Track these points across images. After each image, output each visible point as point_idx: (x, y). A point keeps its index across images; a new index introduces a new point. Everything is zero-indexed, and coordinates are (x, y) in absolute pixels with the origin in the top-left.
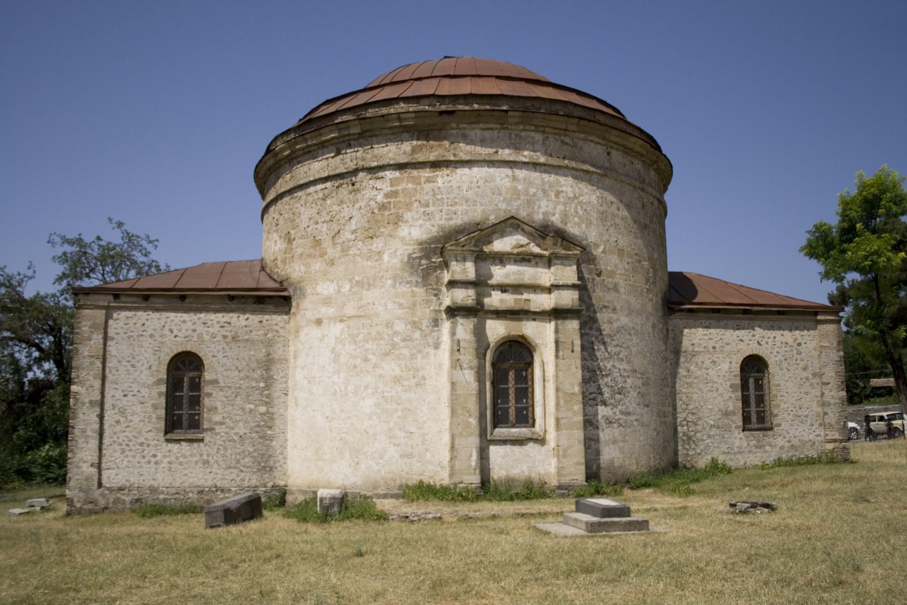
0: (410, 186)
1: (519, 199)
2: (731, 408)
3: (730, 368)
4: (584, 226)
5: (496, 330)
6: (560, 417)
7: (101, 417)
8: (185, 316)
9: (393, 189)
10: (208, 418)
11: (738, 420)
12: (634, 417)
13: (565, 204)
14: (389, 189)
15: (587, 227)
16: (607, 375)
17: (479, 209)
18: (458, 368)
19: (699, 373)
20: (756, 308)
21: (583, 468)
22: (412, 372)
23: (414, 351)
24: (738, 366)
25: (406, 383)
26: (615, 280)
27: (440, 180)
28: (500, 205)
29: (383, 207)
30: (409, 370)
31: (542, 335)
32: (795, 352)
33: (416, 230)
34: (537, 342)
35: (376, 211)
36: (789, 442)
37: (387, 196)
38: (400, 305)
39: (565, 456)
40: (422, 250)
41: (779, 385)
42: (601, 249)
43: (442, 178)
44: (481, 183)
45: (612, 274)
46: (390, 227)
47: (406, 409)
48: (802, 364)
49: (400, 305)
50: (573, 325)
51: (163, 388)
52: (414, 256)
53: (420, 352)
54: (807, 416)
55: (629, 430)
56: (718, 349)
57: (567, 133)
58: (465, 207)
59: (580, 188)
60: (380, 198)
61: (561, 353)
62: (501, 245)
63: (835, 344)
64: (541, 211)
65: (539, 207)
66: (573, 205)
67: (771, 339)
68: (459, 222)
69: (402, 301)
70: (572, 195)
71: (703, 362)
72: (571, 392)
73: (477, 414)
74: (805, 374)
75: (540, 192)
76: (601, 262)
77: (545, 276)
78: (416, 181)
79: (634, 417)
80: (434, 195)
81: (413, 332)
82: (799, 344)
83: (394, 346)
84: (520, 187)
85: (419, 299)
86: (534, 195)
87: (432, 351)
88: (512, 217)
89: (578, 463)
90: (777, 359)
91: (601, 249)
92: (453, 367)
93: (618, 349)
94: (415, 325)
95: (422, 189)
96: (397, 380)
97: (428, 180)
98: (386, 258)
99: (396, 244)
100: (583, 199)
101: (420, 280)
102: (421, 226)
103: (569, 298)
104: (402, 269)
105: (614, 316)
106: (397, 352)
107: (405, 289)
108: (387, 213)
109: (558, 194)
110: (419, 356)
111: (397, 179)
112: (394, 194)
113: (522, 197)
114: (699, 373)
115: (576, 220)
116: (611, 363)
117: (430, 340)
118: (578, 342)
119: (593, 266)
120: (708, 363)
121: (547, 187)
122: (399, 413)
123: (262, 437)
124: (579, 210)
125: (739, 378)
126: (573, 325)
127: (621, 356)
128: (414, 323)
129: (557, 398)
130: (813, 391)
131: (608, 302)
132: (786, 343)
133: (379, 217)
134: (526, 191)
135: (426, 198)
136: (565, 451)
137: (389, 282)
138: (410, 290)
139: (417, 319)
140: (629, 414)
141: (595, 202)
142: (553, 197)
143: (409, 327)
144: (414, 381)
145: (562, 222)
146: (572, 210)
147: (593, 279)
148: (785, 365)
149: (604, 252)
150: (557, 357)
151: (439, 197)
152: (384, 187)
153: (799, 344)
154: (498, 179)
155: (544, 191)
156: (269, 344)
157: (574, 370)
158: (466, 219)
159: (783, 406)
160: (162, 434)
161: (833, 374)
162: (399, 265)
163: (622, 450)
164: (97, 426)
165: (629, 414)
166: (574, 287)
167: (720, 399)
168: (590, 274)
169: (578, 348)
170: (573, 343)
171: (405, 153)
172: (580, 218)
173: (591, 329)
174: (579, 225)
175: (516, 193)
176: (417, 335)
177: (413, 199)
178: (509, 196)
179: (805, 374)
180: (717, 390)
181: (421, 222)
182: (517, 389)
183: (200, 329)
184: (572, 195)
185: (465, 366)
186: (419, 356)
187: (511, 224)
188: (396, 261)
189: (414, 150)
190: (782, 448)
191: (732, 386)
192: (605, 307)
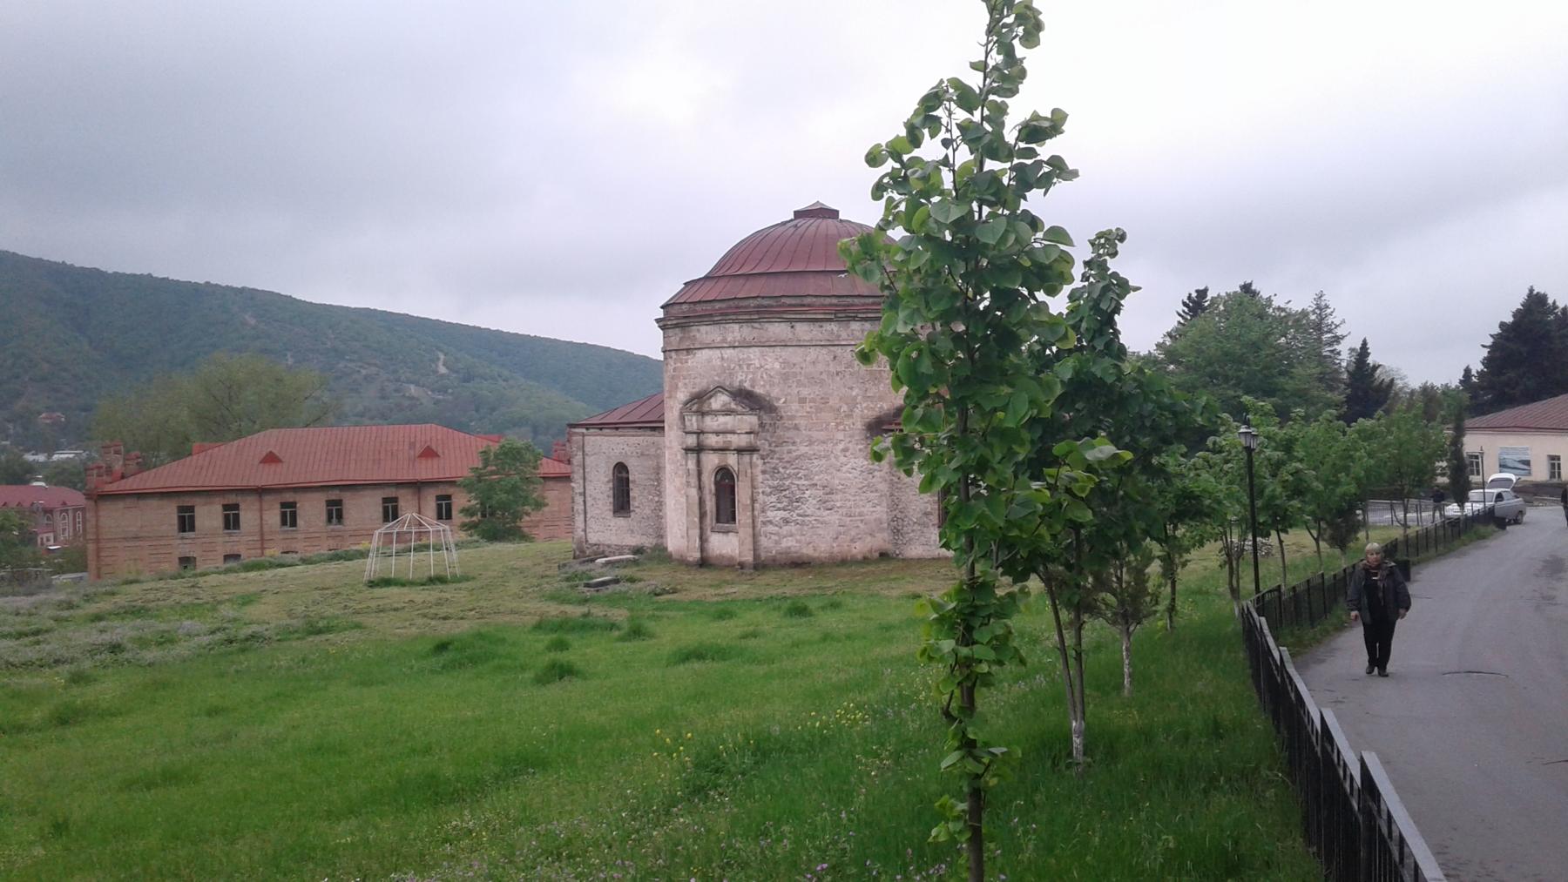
8: (618, 439)
10: (634, 504)
11: (935, 519)
45: (792, 418)
175: (724, 370)
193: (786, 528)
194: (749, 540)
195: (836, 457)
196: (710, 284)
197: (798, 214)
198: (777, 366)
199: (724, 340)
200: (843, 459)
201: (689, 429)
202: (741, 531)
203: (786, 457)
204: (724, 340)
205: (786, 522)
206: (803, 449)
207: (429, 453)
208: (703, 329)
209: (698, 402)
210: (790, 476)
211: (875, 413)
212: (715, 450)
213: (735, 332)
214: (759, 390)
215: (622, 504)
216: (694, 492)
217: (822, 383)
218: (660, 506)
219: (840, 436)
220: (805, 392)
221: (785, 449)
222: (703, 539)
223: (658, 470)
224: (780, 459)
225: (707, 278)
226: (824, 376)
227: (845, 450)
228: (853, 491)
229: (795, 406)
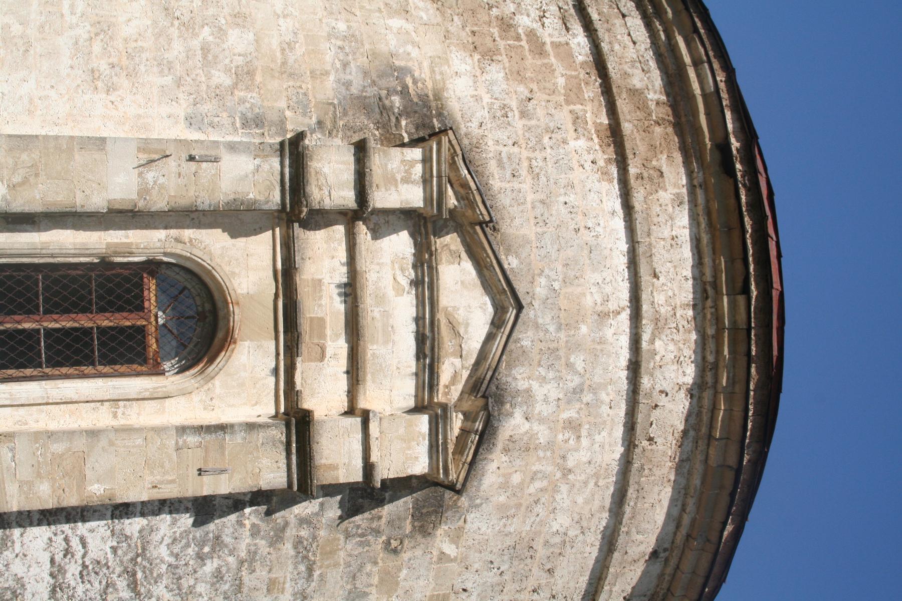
0: (561, 81)
1: (559, 329)
4: (502, 499)
5: (244, 266)
6: (19, 443)
9: (548, 47)
14: (548, 40)
15: (501, 508)
16: (133, 586)
17: (529, 231)
18: (144, 157)
22: (125, 62)
23: (179, 69)
25: (97, 47)
27: (582, 143)
28: (543, 281)
29: (506, 25)
30: (130, 57)
31: (241, 386)
33: (469, 90)
34: (217, 382)
35: (495, 12)
37: (531, 35)
38: (290, 46)
40: (424, 98)
42: (450, 549)
43: (586, 150)
44: (586, 236)
46: (465, 36)
47: (28, 45)
49: (290, 46)
50: (273, 472)
52: (409, 81)
53: (179, 83)
57: (702, 445)
58: (530, 197)
59: (586, 483)
60: (524, 22)
61: (192, 439)
62: (457, 277)
64: (535, 385)
65: (543, 380)
66: (549, 469)
69: (300, 50)
70: (570, 464)
72: (89, 473)
75: (577, 380)
76: (418, 552)
77: (392, 386)
78: (573, 94)
80: (548, 130)
81: (227, 70)
83: (189, 27)
84: (584, 329)
85: (308, 85)
86: (569, 366)
87: (182, 109)
88: (520, 307)
91: (450, 549)
92: (144, 146)
94: (244, 75)
95: (558, 106)
96: (103, 29)
97: (577, 120)
98: (396, 23)
99: (431, 46)
100: (563, 497)
101: (354, 90)
102: (477, 99)
103: (339, 455)
104: (374, 55)
106: (174, 32)
107: (330, 56)
108: (495, 31)
109: (573, 426)
110: (168, 80)
111: (570, 55)
112: (539, 49)
113: (562, 335)
115: (516, 479)
117: (206, 107)
119: (408, 528)
121: (588, 397)
122: (17, 29)
124: (538, 484)
126: (273, 472)
128: (251, 73)
129: (70, 434)
133: (483, 16)
134: (574, 346)
135: (540, 112)
137: (342, 26)
138: (328, 67)
139: (258, 78)
141: (555, 527)
142: (565, 415)
143: (240, 61)
144: (103, 66)
145: (511, 439)
146: (536, 467)
147: (377, 532)
149: (443, 557)
150: (182, 430)
151: (546, 140)
152: (548, 31)
154: (597, 277)
155: (578, 391)
157: (149, 479)
158: (504, 200)
162: (382, 48)
166: (368, 468)
168: (390, 523)
170: (223, 471)
171: (626, 75)
172: (521, 486)
173: (255, 532)
174: (505, 486)
176: (221, 78)
177: (534, 86)
178: (563, 303)
181: (487, 99)
182: (87, 332)
184: (570, 464)
185: (150, 176)
186: (168, 80)
187: (507, 300)
188: (393, 42)
192: (310, 570)
198: (561, 522)
216: (119, 185)
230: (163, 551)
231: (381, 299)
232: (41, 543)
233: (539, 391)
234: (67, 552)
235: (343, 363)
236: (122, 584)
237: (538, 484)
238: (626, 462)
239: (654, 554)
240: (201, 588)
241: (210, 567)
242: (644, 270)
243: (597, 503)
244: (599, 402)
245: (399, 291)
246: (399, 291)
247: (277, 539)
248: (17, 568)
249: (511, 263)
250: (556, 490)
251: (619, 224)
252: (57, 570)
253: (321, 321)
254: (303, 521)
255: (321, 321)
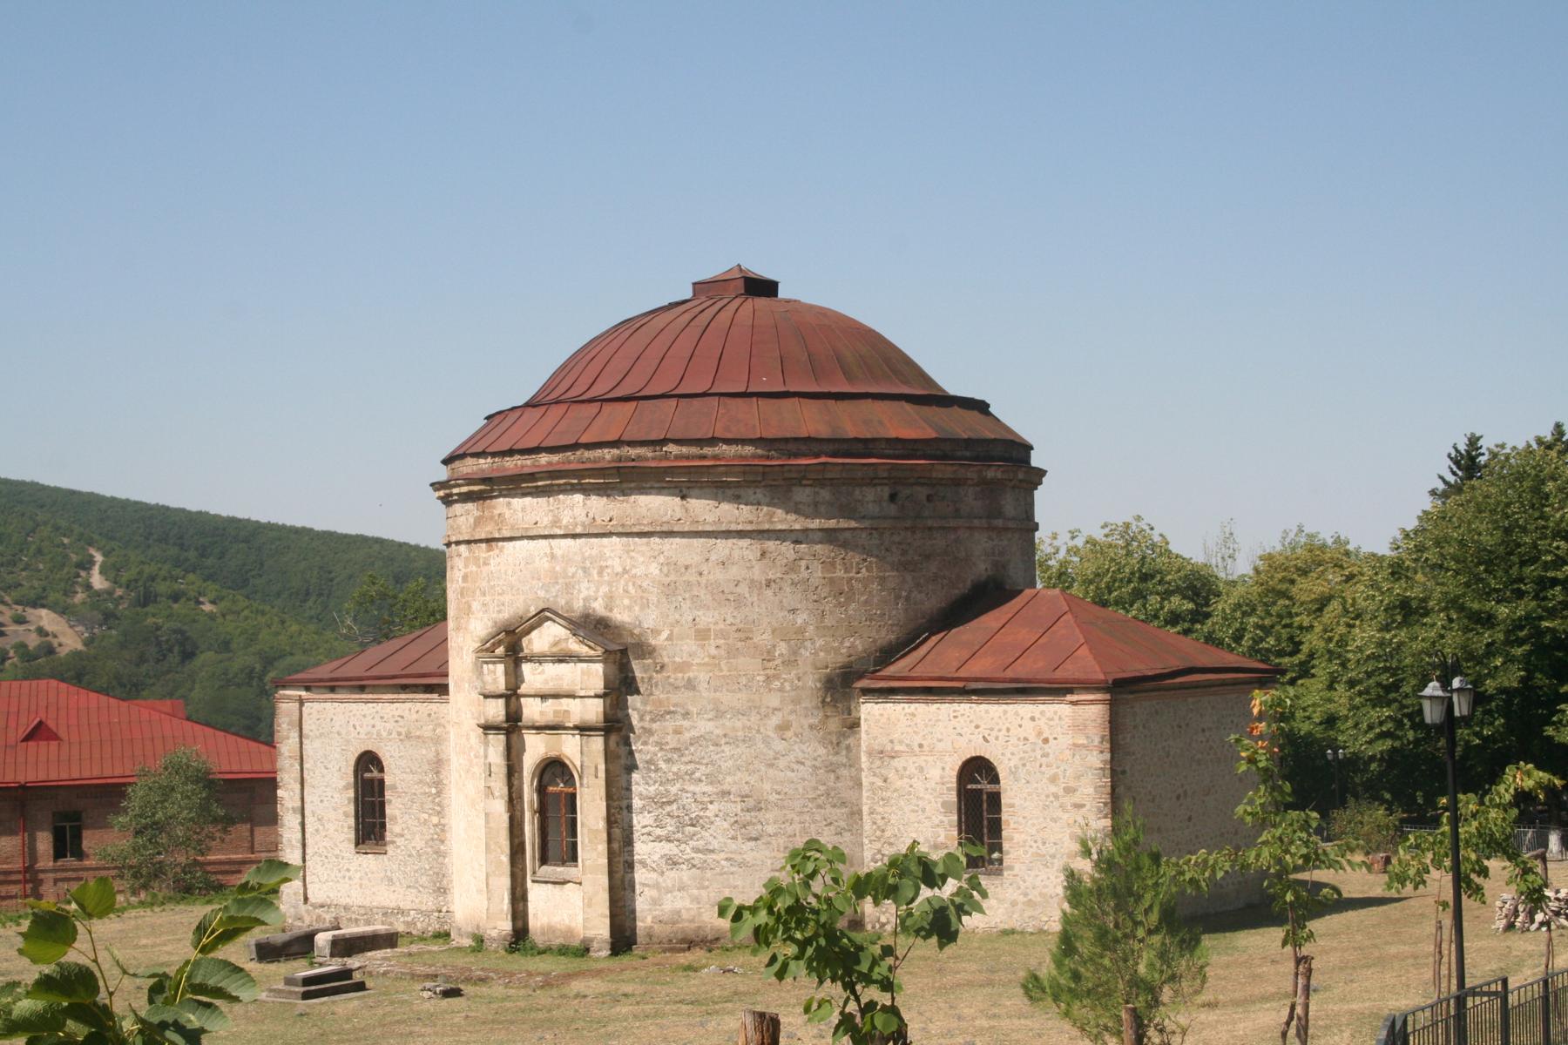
2: (941, 839)
3: (942, 777)
5: (535, 748)
7: (303, 825)
10: (392, 829)
12: (723, 855)
13: (610, 584)
15: (642, 608)
16: (670, 803)
17: (522, 598)
19: (899, 783)
20: (974, 685)
21: (607, 921)
24: (955, 774)
26: (691, 675)
32: (1039, 753)
36: (1026, 895)
39: (589, 906)
41: (1012, 806)
45: (683, 667)
48: (1051, 772)
51: (351, 793)
54: (1053, 856)
55: (709, 874)
56: (926, 748)
63: (1097, 740)
67: (1004, 732)
68: (507, 616)
70: (620, 570)
71: (905, 769)
73: (507, 850)
74: (1053, 789)
79: (723, 855)
82: (1046, 741)
89: (602, 915)
90: (1012, 764)
91: (665, 635)
93: (690, 767)
105: (686, 723)
114: (899, 783)
115: (626, 602)
116: (678, 786)
118: (602, 767)
120: (912, 769)
121: (588, 564)
123: (437, 852)
124: (631, 588)
125: (954, 793)
127: (697, 775)
130: (1065, 816)
131: (675, 705)
132: (1026, 739)
136: (590, 899)
140: (712, 851)
147: (650, 678)
148: (1022, 773)
149: (670, 638)
153: (1046, 741)
155: (585, 570)
156: (438, 740)
159: (1017, 837)
160: (353, 846)
161: (1091, 790)
163: (696, 900)
164: (299, 835)
165: (712, 851)
167: (927, 823)
169: (602, 774)
172: (631, 598)
173: (645, 743)
174: (630, 608)
179: (1053, 789)
180: (924, 810)
183: (379, 725)
187: (541, 617)
189: (478, 522)
190: (1014, 904)
191: (944, 804)
192: (669, 713)
193: (672, 875)
194: (603, 898)
195: (766, 741)
196: (536, 413)
197: (698, 286)
198: (654, 569)
199: (556, 522)
200: (779, 746)
201: (491, 688)
202: (587, 880)
203: (673, 742)
204: (556, 522)
205: (673, 862)
206: (704, 726)
207: (39, 732)
208: (517, 502)
209: (509, 644)
210: (678, 777)
211: (842, 660)
212: (540, 729)
213: (576, 508)
214: (620, 616)
215: (370, 826)
217: (739, 602)
218: (440, 835)
219: (774, 700)
220: (706, 618)
221: (670, 724)
222: (519, 898)
223: (438, 764)
224: (660, 745)
225: (530, 405)
226: (743, 589)
227: (783, 727)
228: (797, 805)
229: (689, 645)
230: (652, 789)
231: (546, 682)
232: (644, 846)
233: (584, 593)
234: (649, 834)
235: (570, 700)
236: (668, 808)
237: (631, 588)
238: (619, 535)
239: (683, 498)
240: (675, 769)
241: (663, 765)
242: (534, 533)
243: (644, 548)
244: (590, 557)
245: (543, 672)
246: (543, 672)
247: (650, 732)
248: (656, 857)
249: (533, 611)
250: (634, 576)
251: (518, 543)
252: (659, 839)
253: (556, 712)
254: (641, 719)
255: (556, 712)
